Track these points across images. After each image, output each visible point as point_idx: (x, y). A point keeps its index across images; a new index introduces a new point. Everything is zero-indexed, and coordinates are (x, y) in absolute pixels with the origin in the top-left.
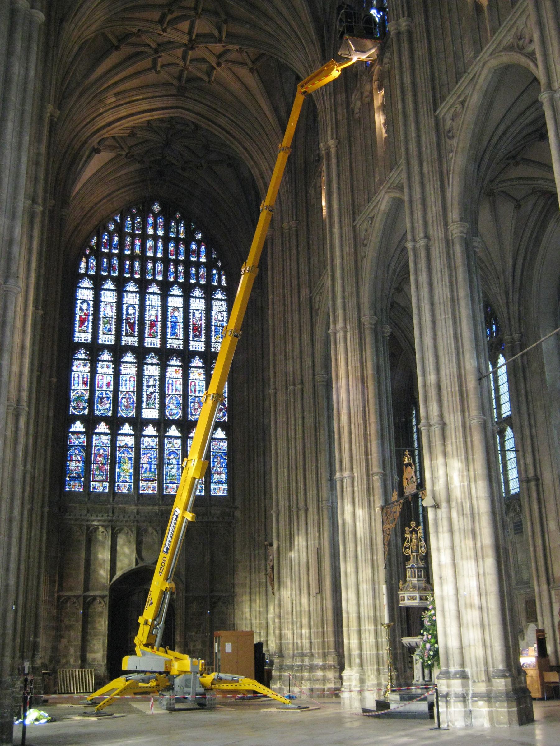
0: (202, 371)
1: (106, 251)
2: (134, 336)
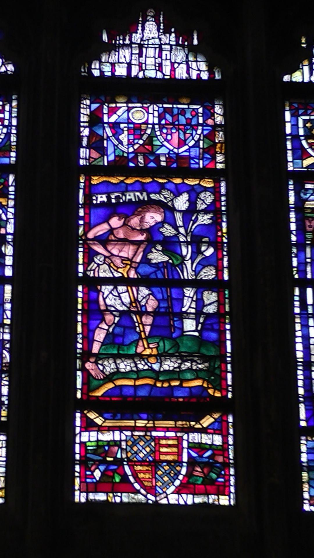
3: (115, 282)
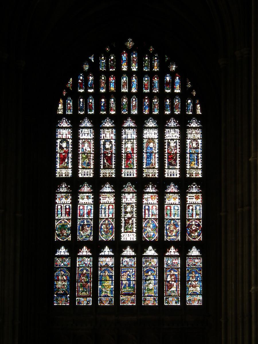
0: (177, 196)
1: (82, 91)
2: (112, 168)
3: (124, 280)
